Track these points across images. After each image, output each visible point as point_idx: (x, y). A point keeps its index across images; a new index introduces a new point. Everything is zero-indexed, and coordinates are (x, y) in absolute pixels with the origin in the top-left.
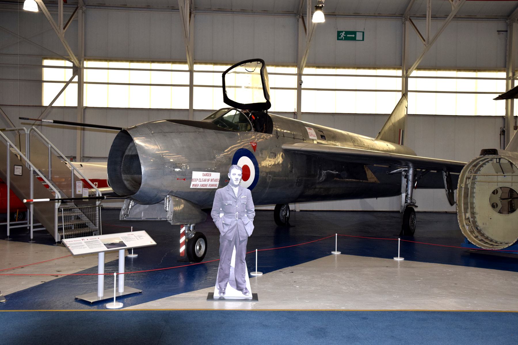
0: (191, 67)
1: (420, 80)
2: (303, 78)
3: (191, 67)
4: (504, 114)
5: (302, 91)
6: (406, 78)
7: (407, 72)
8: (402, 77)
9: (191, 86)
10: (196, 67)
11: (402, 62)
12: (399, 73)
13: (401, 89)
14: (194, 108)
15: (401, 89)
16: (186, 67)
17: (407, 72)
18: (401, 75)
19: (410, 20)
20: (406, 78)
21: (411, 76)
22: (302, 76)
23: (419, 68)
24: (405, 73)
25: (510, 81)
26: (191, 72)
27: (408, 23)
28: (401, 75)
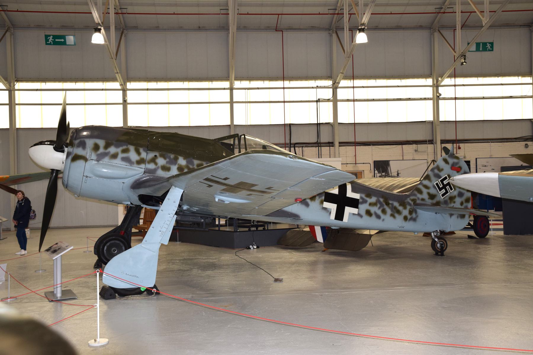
0: (231, 84)
3: (231, 84)
5: (338, 103)
9: (232, 102)
10: (237, 84)
13: (431, 97)
14: (235, 124)
15: (431, 97)
16: (227, 84)
17: (437, 81)
18: (431, 84)
19: (439, 31)
21: (442, 84)
24: (435, 82)
26: (231, 89)
27: (436, 34)
28: (431, 84)
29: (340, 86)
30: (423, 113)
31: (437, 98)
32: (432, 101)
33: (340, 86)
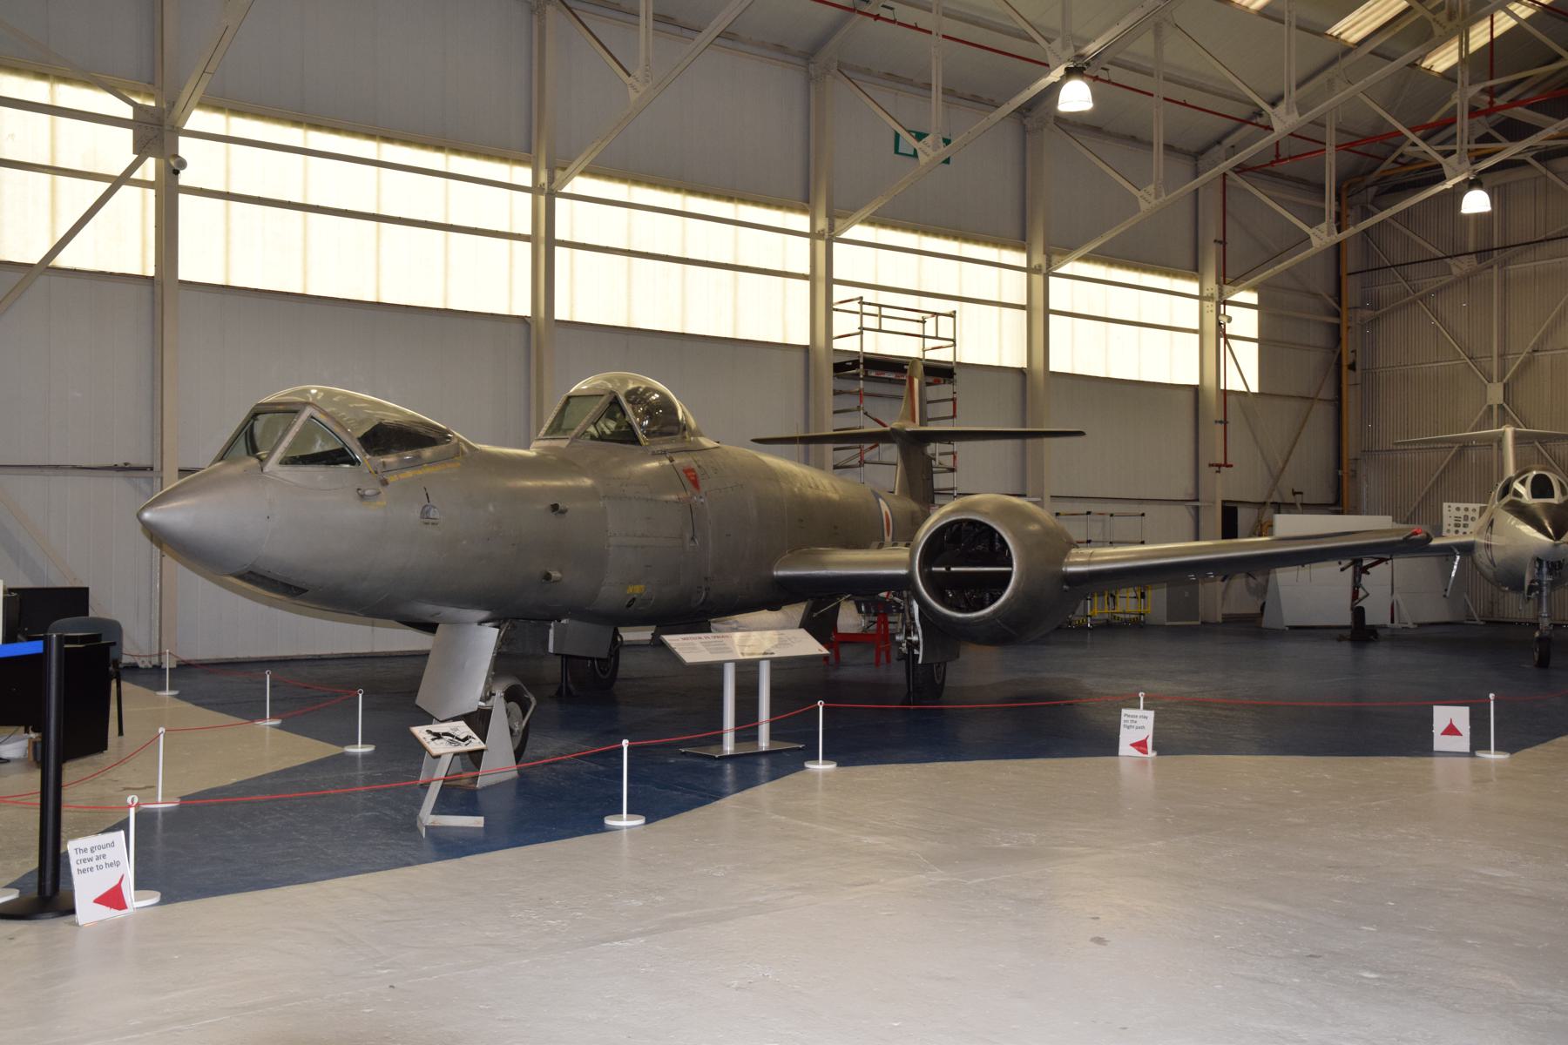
1: (594, 210)
2: (186, 147)
4: (805, 340)
6: (546, 194)
7: (551, 179)
8: (535, 190)
11: (546, 142)
12: (523, 175)
13: (528, 231)
15: (528, 231)
18: (528, 183)
20: (546, 194)
21: (566, 189)
22: (182, 140)
23: (592, 172)
24: (543, 178)
25: (821, 245)
27: (553, 14)
29: (188, 126)
30: (494, 284)
32: (528, 245)
33: (188, 126)
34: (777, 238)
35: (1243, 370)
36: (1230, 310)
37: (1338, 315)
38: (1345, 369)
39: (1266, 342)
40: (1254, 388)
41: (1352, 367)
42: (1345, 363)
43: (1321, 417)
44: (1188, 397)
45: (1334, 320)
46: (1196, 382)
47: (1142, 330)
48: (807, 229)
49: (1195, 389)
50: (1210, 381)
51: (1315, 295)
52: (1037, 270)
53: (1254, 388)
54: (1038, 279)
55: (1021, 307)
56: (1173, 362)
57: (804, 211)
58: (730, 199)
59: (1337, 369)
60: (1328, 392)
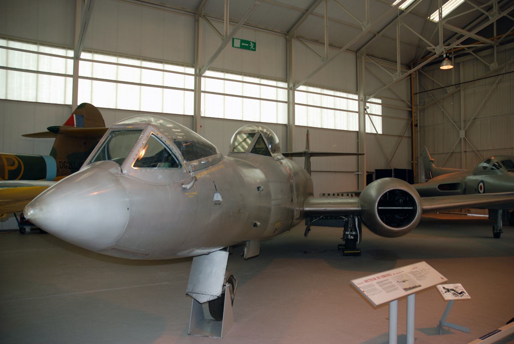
31: (197, 91)
34: (182, 77)
35: (375, 125)
36: (368, 105)
37: (411, 108)
38: (414, 126)
39: (384, 116)
40: (380, 132)
41: (416, 125)
42: (413, 124)
43: (405, 143)
44: (355, 135)
45: (410, 109)
46: (357, 130)
47: (333, 111)
48: (193, 73)
49: (357, 132)
50: (362, 130)
51: (404, 101)
52: (291, 89)
53: (380, 132)
54: (291, 92)
55: (286, 102)
56: (349, 123)
57: (192, 66)
58: (161, 62)
59: (412, 126)
60: (408, 134)
